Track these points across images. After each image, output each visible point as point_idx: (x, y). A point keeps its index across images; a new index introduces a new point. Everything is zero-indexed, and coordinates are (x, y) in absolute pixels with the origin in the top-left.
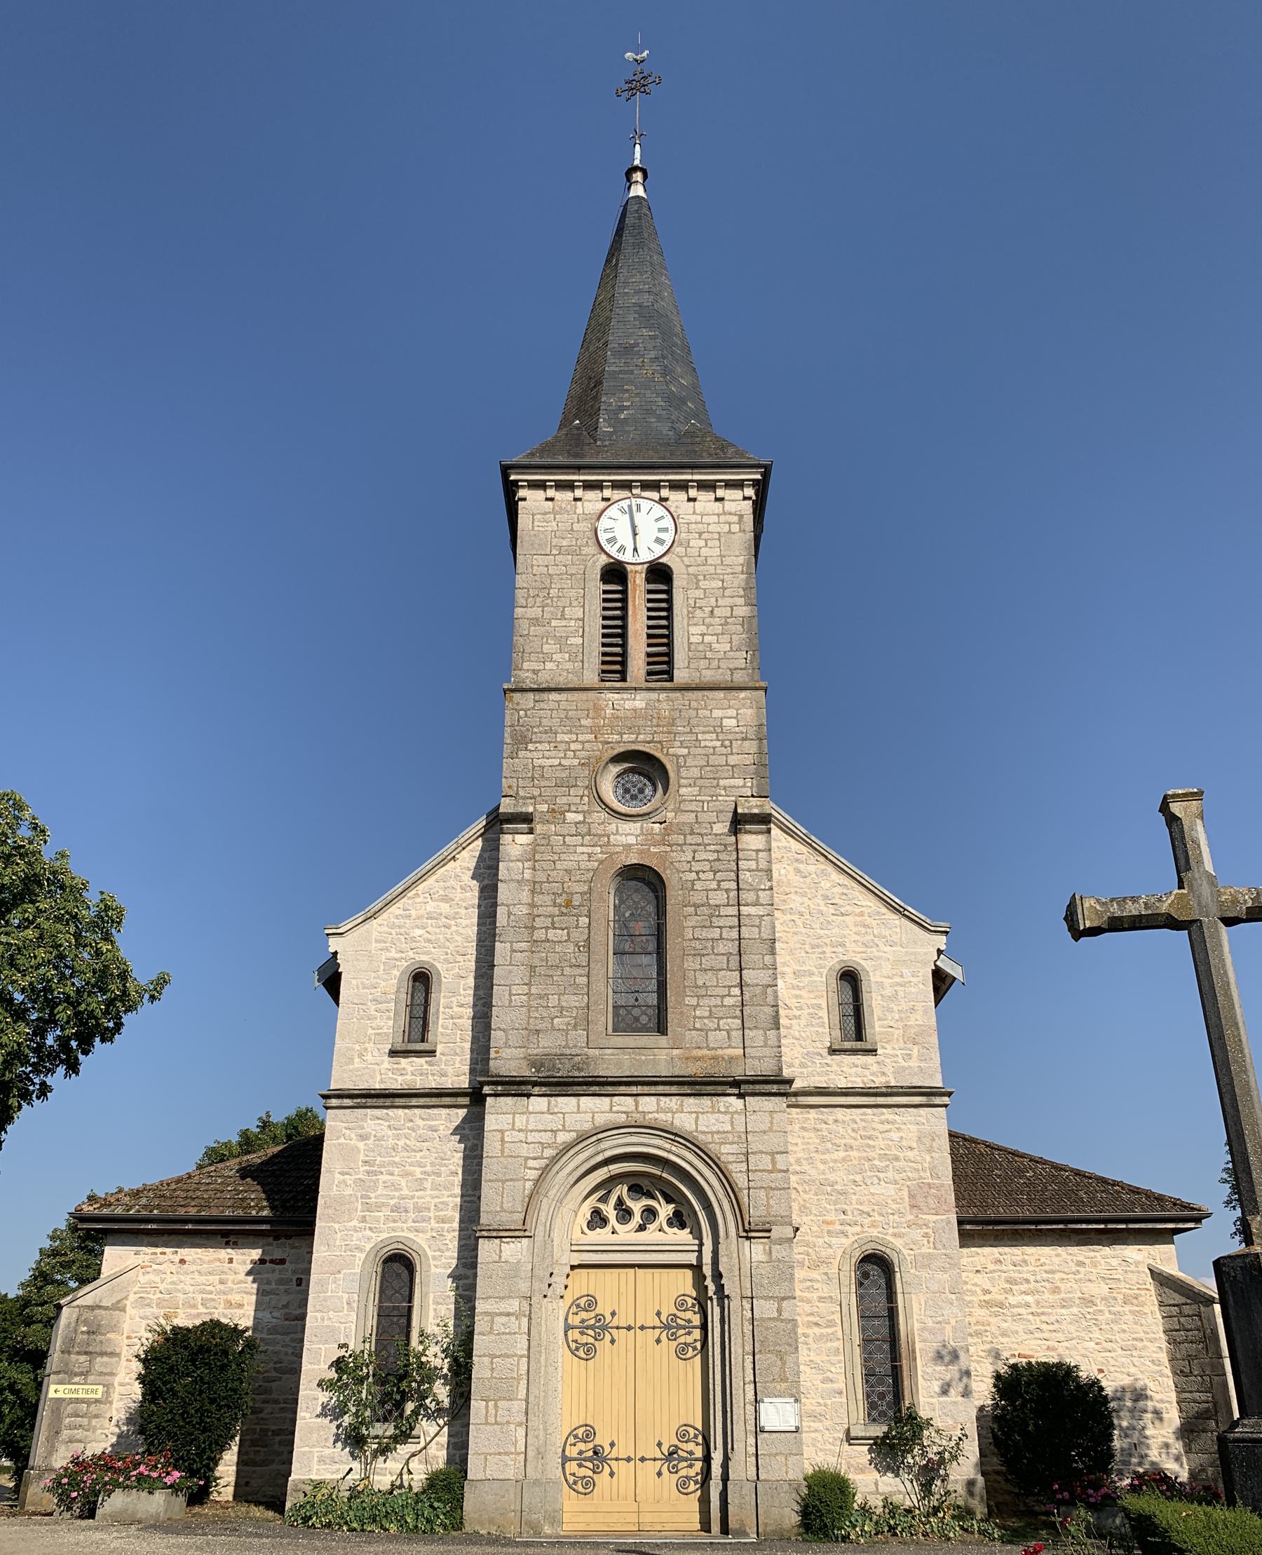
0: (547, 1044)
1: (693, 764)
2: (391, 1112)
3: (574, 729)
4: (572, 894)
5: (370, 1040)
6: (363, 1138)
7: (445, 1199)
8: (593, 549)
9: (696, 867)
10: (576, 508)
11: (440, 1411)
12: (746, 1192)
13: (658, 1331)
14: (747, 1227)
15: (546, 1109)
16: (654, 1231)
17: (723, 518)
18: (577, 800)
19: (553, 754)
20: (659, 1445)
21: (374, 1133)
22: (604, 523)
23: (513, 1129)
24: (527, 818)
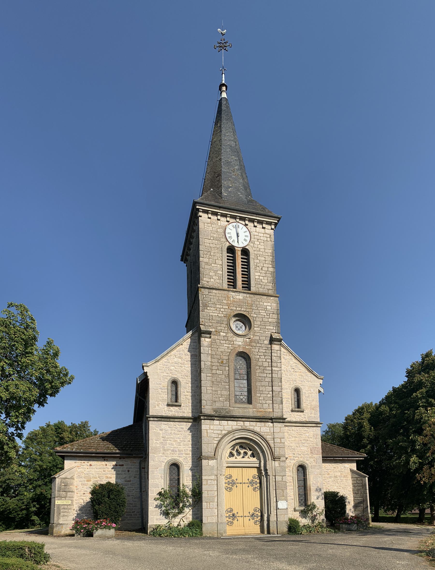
0: (218, 405)
1: (258, 320)
2: (169, 423)
4: (223, 359)
6: (161, 430)
7: (187, 448)
9: (259, 354)
11: (190, 506)
12: (273, 448)
13: (248, 484)
15: (218, 424)
17: (265, 235)
18: (224, 328)
20: (249, 513)
23: (210, 429)
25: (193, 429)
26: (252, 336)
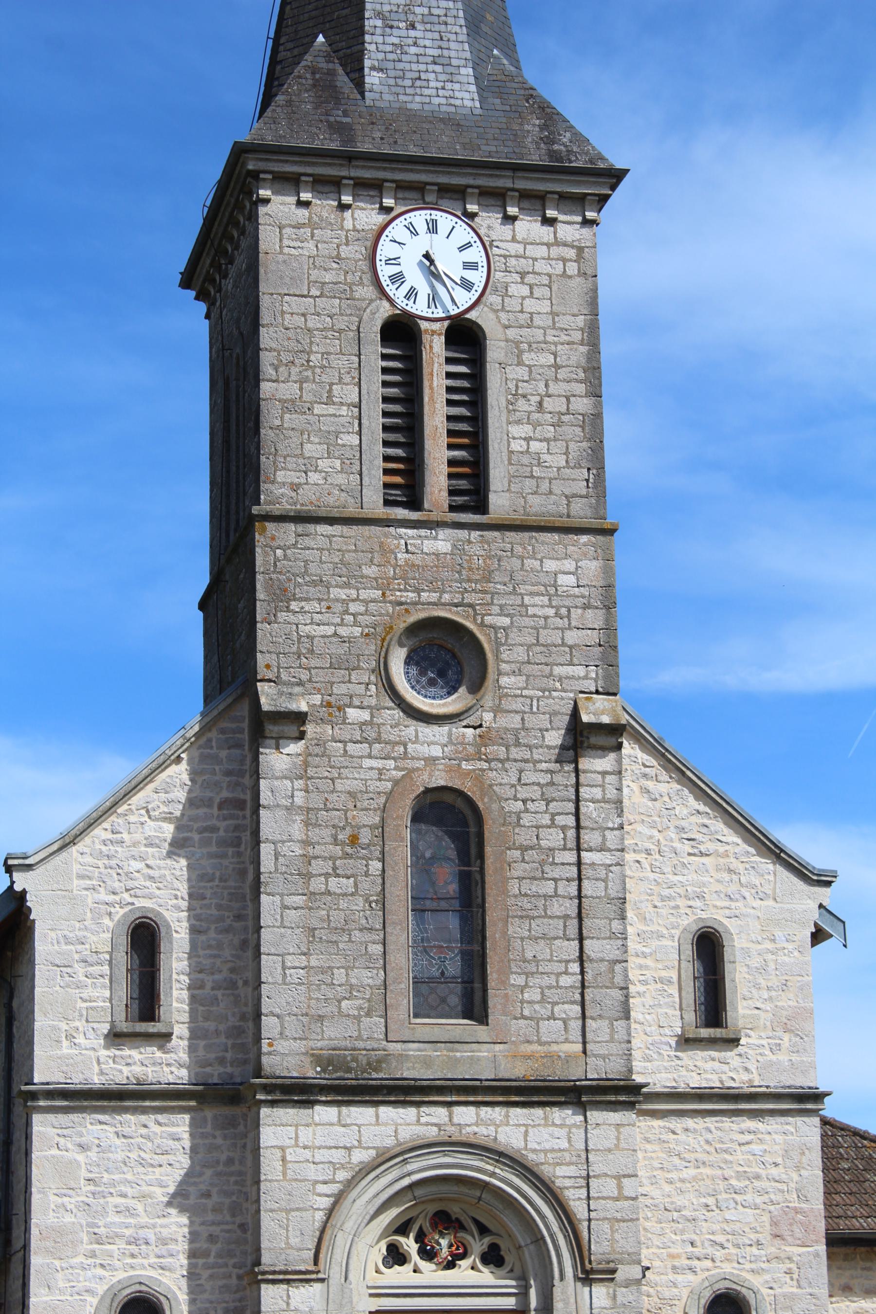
1: (518, 640)
3: (353, 581)
4: (359, 828)
5: (81, 1015)
6: (83, 1147)
8: (367, 291)
10: (343, 219)
12: (586, 1224)
14: (588, 1267)
15: (336, 1120)
16: (466, 1269)
17: (555, 251)
19: (325, 618)
21: (97, 1141)
22: (385, 249)
23: (297, 1146)
24: (300, 718)
25: (225, 1137)
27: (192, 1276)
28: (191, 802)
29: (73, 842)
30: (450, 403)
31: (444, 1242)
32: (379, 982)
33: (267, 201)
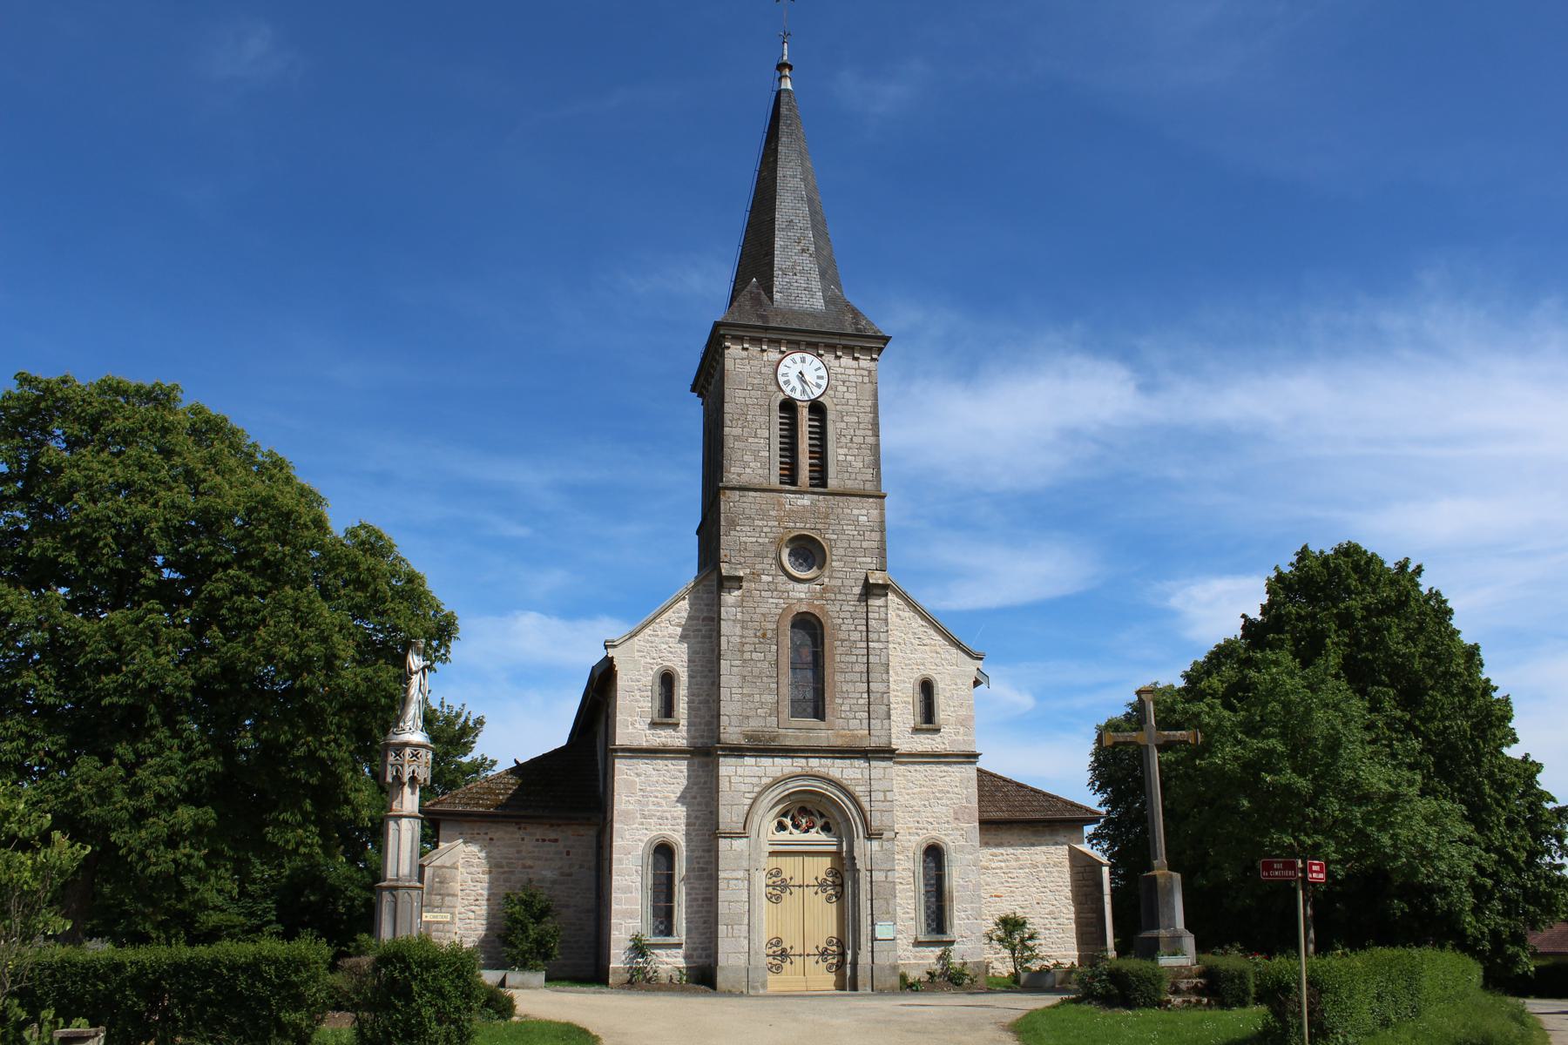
0: (754, 724)
6: (638, 775)
8: (773, 388)
17: (858, 372)
20: (817, 947)
22: (781, 369)
24: (740, 579)
26: (826, 580)
27: (687, 834)
28: (690, 618)
29: (635, 635)
30: (810, 438)
31: (804, 821)
32: (775, 701)
33: (729, 348)
